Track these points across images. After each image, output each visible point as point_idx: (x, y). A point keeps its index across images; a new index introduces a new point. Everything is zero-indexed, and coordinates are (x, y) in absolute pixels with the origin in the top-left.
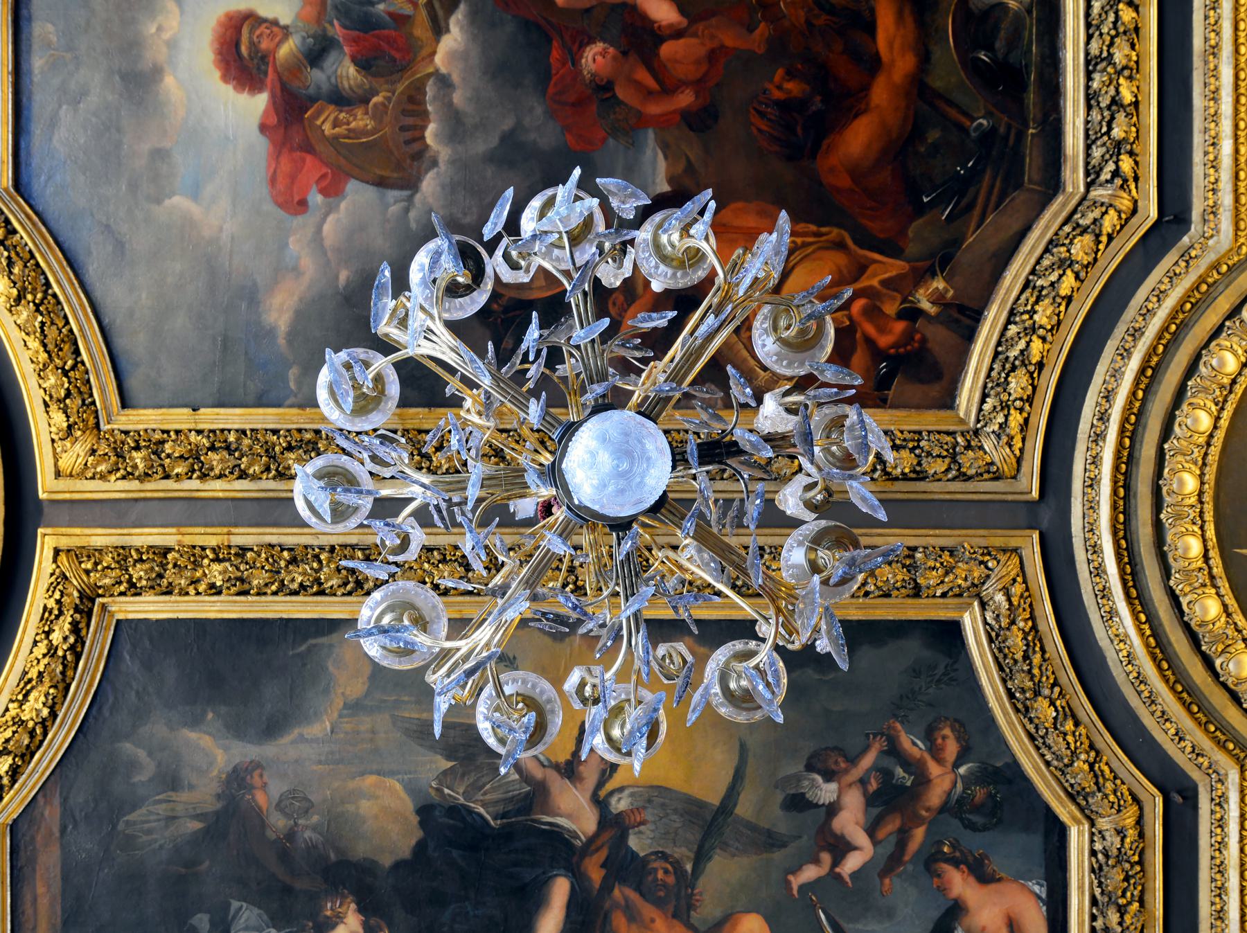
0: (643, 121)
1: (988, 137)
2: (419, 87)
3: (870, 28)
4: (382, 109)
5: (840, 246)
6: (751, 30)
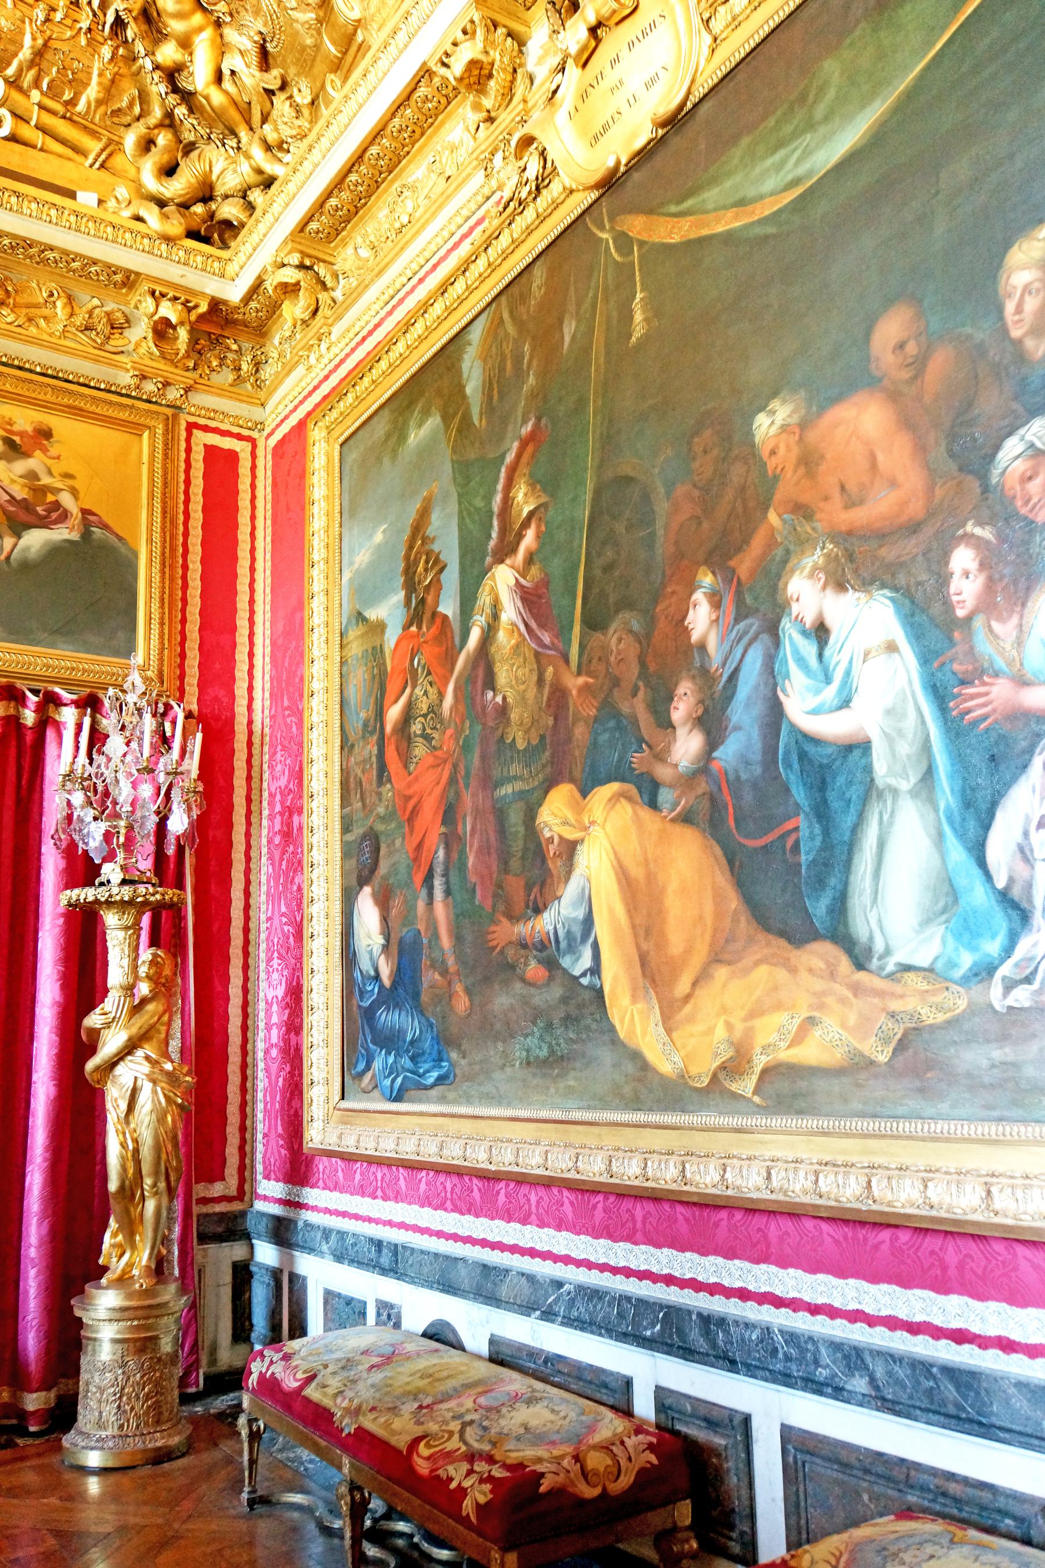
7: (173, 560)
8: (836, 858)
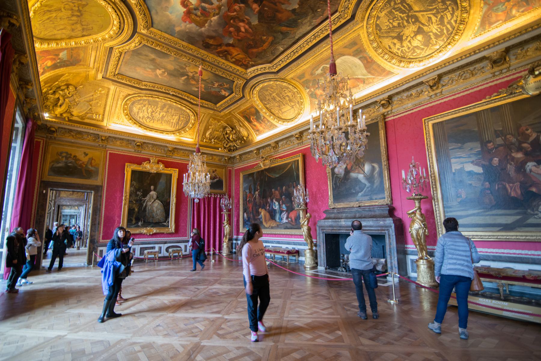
0: (233, 37)
2: (208, 20)
7: (226, 182)
8: (275, 215)
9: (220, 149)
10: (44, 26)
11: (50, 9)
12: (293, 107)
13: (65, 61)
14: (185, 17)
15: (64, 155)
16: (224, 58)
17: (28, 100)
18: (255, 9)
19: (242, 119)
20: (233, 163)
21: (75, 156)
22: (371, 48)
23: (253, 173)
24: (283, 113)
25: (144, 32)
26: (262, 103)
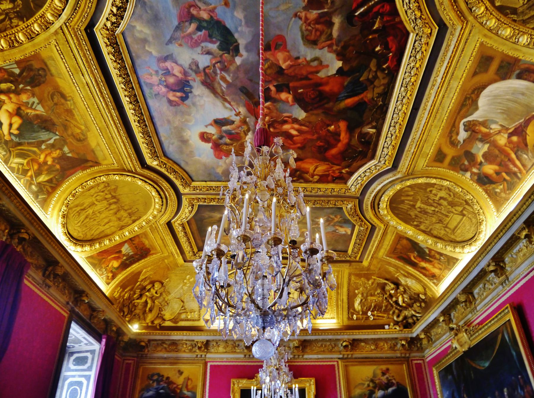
1: (360, 151)
3: (339, 135)
4: (236, 146)
5: (328, 164)
6: (313, 135)
9: (387, 327)
10: (86, 226)
11: (82, 208)
12: (464, 215)
13: (132, 256)
14: (217, 153)
15: (156, 377)
16: (302, 181)
17: (95, 314)
18: (287, 98)
19: (400, 264)
20: (421, 349)
21: (168, 378)
22: (525, 49)
23: (451, 365)
24: (454, 230)
25: (187, 191)
26: (411, 225)
